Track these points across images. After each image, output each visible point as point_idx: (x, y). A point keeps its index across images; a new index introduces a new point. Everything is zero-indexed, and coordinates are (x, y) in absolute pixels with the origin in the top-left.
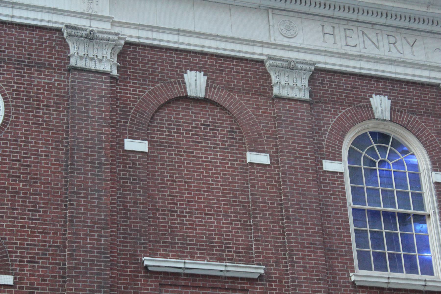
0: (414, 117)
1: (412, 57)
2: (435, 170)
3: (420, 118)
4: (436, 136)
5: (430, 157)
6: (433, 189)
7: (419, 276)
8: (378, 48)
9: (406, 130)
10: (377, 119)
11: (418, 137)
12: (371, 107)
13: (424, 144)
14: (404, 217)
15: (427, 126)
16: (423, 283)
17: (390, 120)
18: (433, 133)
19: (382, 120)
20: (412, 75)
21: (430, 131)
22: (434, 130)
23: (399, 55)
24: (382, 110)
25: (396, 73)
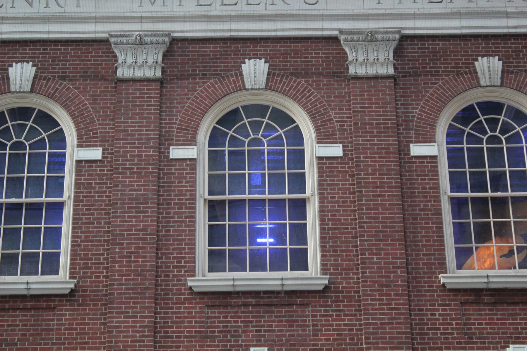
0: (65, 83)
1: (78, 10)
2: (79, 146)
3: (72, 84)
4: (90, 104)
5: (77, 130)
6: (74, 169)
7: (39, 278)
8: (31, 5)
9: (52, 102)
10: (14, 92)
11: (66, 107)
12: (8, 78)
13: (73, 116)
14: (34, 209)
15: (80, 92)
16: (25, 286)
17: (32, 91)
18: (87, 100)
19: (21, 92)
20: (71, 32)
21: (83, 98)
22: (90, 96)
23: (62, 10)
24: (21, 80)
25: (49, 33)
